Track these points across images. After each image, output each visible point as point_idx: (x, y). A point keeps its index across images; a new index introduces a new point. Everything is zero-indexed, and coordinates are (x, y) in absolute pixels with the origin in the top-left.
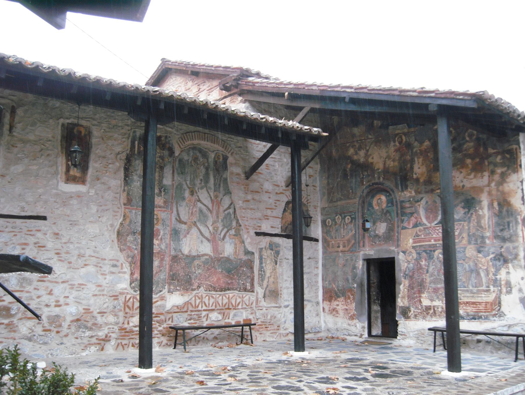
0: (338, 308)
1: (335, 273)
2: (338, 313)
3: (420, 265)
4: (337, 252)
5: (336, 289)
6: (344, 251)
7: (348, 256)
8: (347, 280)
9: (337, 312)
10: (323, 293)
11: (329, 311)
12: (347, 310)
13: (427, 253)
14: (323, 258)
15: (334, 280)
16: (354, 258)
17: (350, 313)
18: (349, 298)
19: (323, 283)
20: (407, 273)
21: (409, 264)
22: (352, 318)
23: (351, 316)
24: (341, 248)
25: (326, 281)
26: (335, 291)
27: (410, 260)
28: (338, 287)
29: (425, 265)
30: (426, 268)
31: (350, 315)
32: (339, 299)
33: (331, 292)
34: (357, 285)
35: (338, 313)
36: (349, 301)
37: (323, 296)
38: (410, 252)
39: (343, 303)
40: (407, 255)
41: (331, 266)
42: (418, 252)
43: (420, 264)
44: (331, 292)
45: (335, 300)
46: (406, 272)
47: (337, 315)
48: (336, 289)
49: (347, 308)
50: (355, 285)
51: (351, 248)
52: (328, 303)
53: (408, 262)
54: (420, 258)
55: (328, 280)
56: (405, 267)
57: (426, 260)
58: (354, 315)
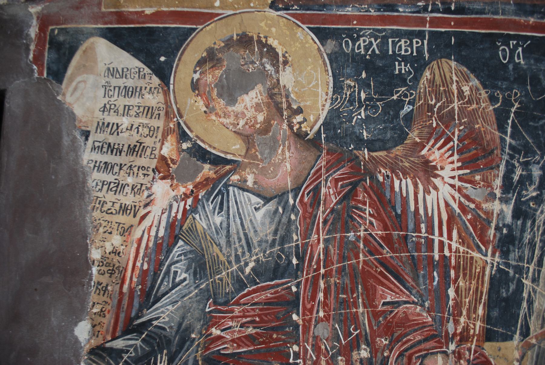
3: (395, 216)
13: (490, 73)
20: (164, 313)
21: (216, 190)
27: (235, 149)
29: (472, 224)
30: (488, 261)
38: (245, 41)
40: (185, 69)
42: (365, 45)
43: (382, 199)
46: (149, 297)
53: (208, 171)
54: (394, 128)
56: (154, 223)
57: (475, 157)
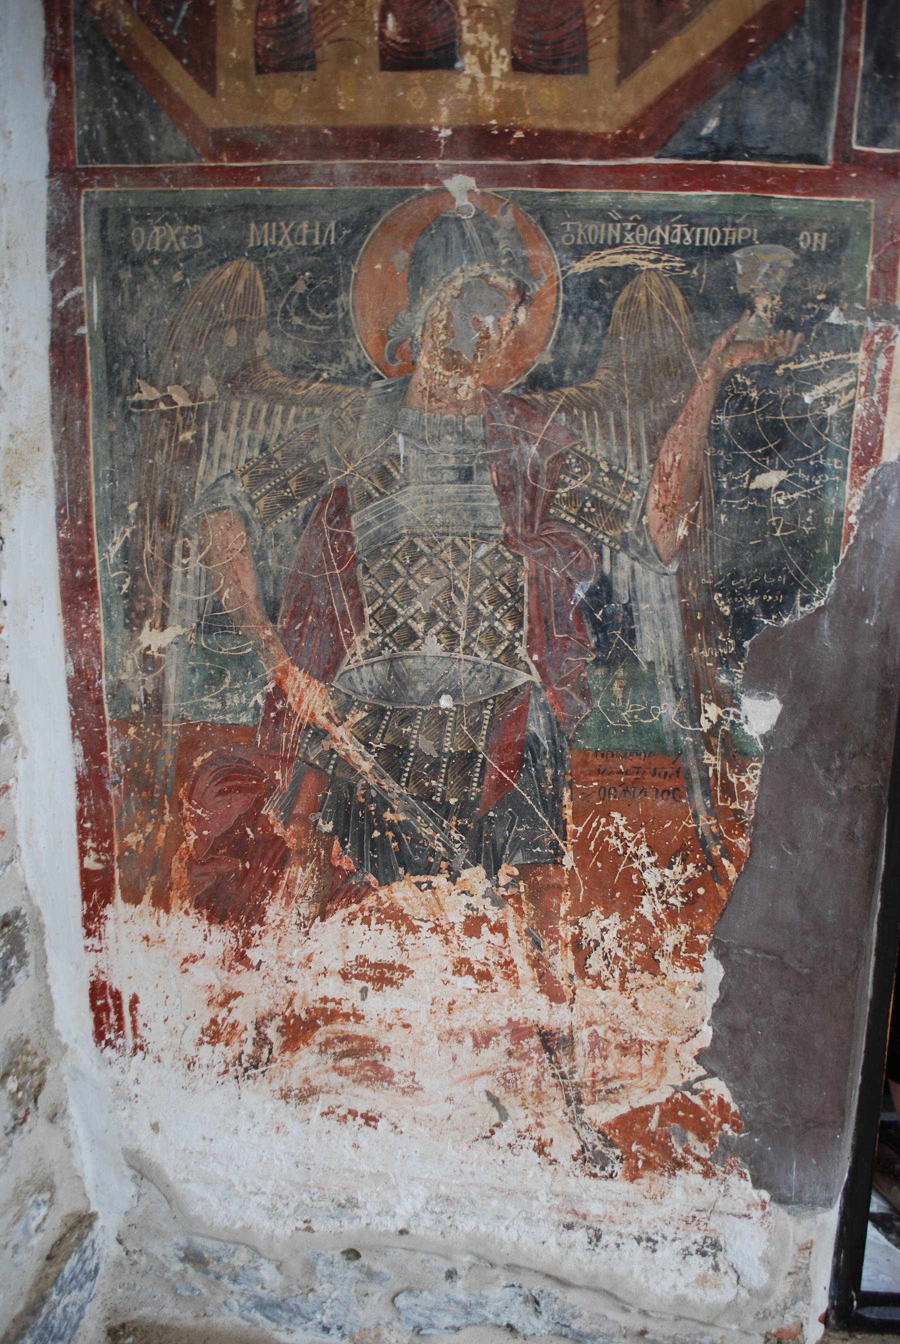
0: (378, 1005)
1: (340, 505)
2: (381, 1076)
4: (401, 140)
5: (345, 740)
6: (543, 142)
7: (636, 233)
8: (607, 624)
9: (363, 1057)
10: (90, 784)
11: (214, 1034)
12: (550, 1042)
14: (61, 238)
15: (315, 611)
16: (764, 271)
17: (605, 1088)
18: (615, 887)
19: (77, 637)
22: (641, 1144)
23: (631, 1125)
24: (483, 76)
25: (134, 619)
26: (338, 779)
28: (386, 714)
31: (602, 1113)
32: (403, 892)
33: (242, 778)
34: (812, 718)
35: (381, 1076)
36: (603, 927)
37: (95, 823)
39: (478, 950)
41: (239, 378)
44: (242, 778)
45: (334, 894)
47: (366, 1098)
48: (345, 740)
49: (559, 1018)
50: (760, 715)
51: (695, 88)
52: (186, 928)
55: (185, 593)
58: (682, 1112)
